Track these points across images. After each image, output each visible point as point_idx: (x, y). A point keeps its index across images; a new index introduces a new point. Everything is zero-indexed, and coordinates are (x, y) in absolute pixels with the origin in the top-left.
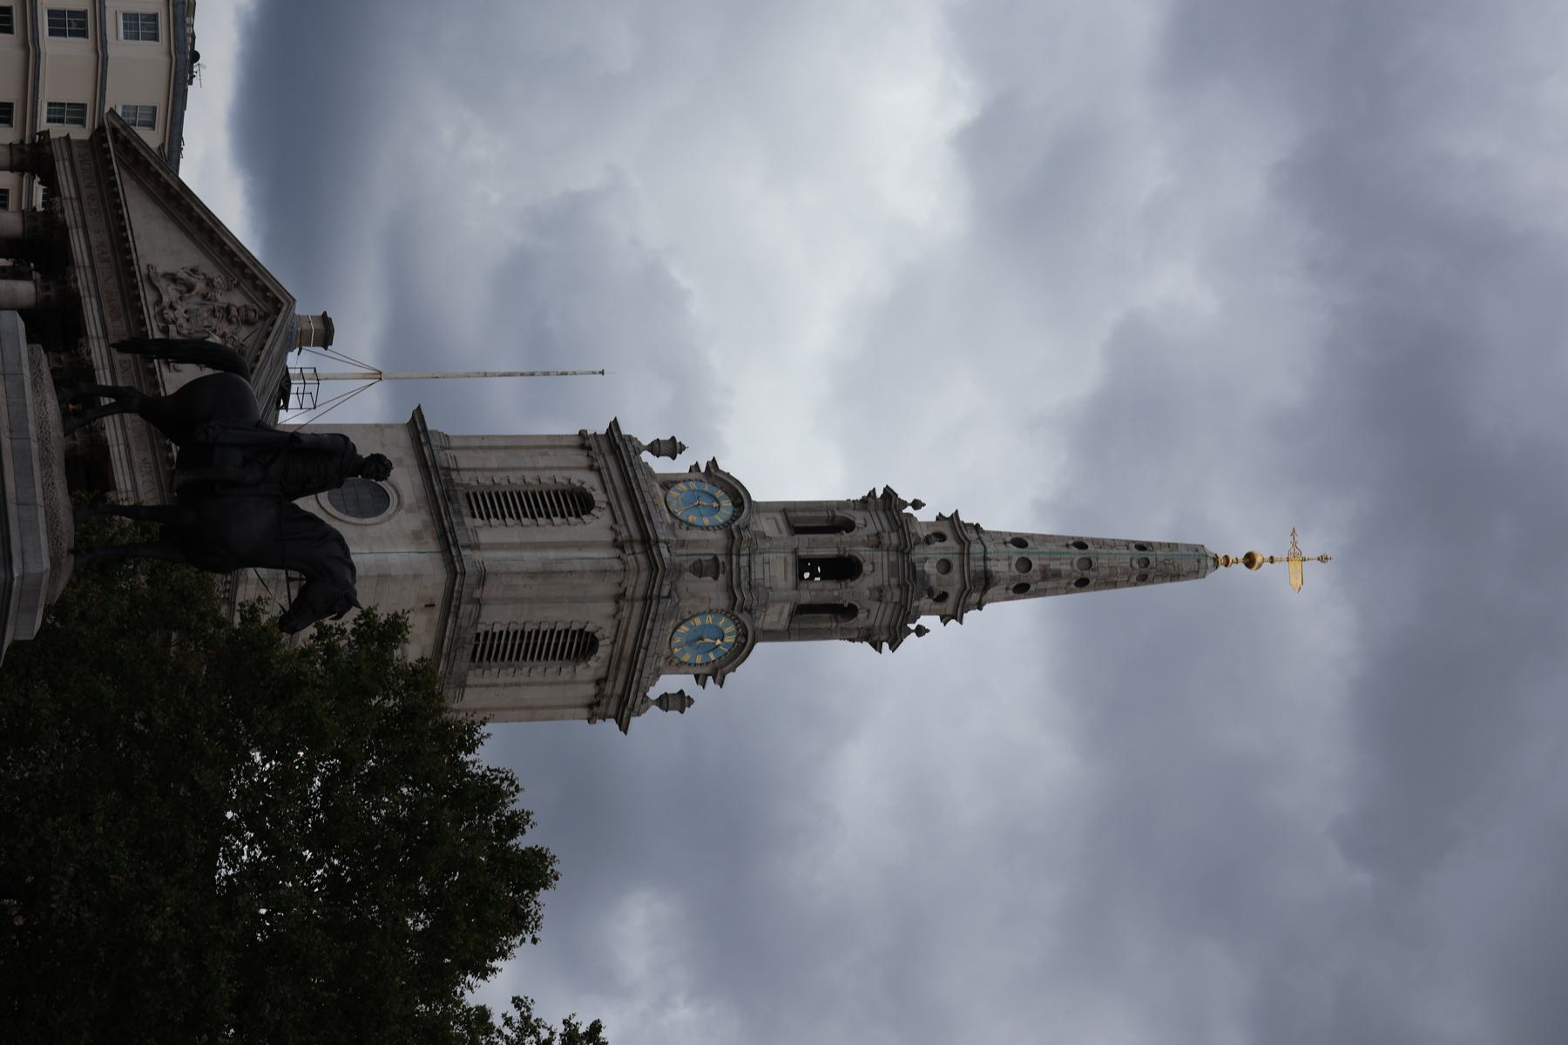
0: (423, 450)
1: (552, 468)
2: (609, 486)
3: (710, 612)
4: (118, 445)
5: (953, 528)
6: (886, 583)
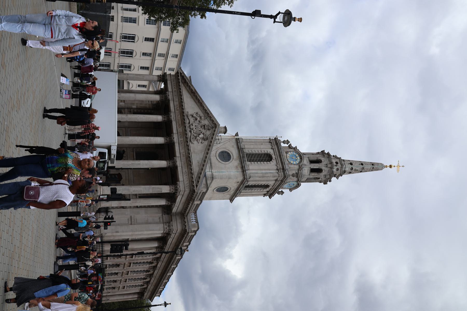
0: (238, 144)
1: (264, 148)
2: (276, 154)
4: (180, 167)
6: (327, 174)
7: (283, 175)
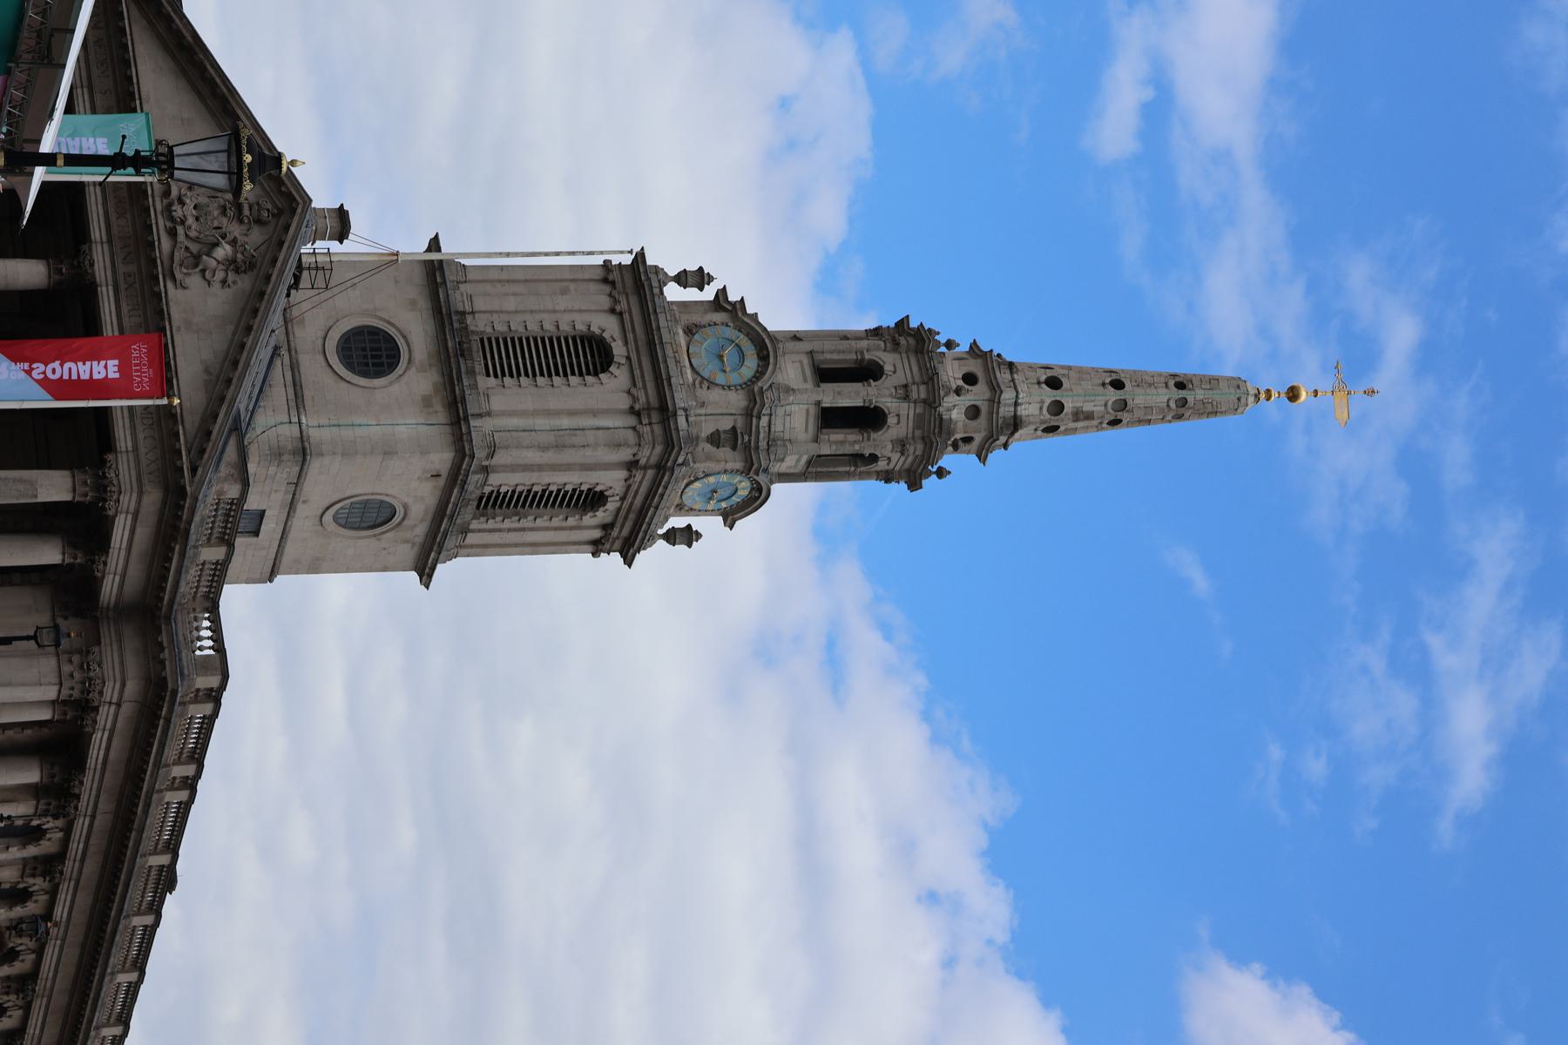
0: (438, 292)
1: (572, 311)
2: (630, 336)
3: (725, 471)
6: (910, 436)
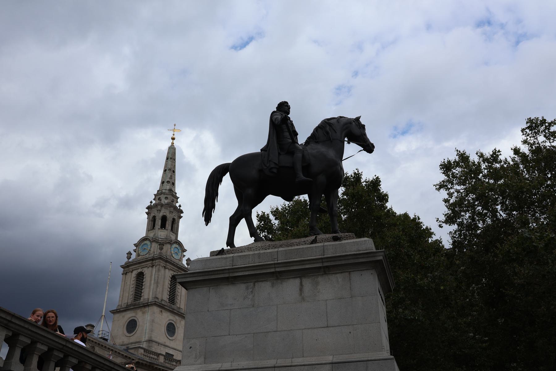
0: (122, 311)
1: (131, 281)
2: (137, 268)
3: (171, 249)
5: (158, 196)
7: (158, 261)
